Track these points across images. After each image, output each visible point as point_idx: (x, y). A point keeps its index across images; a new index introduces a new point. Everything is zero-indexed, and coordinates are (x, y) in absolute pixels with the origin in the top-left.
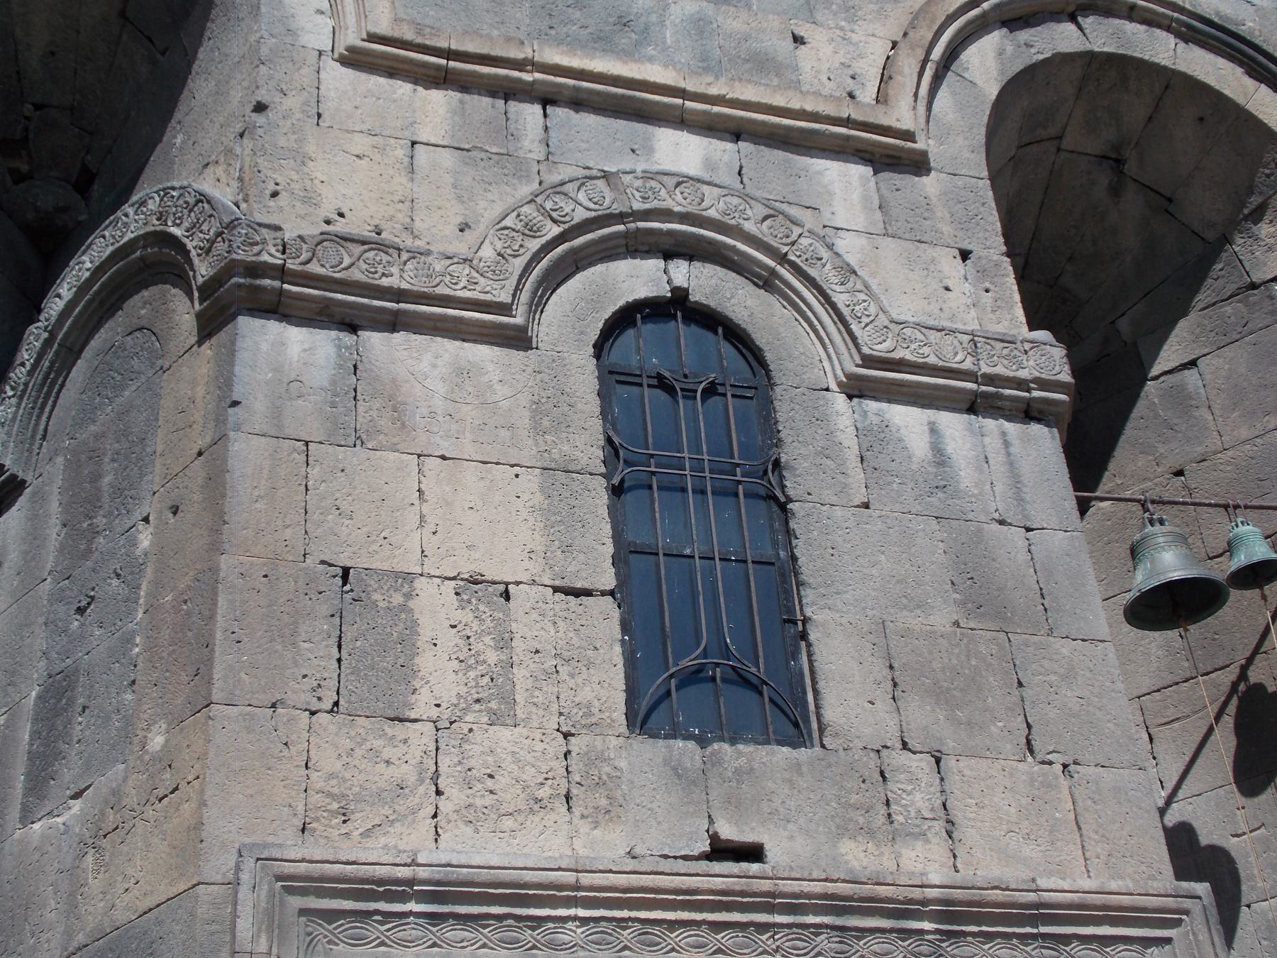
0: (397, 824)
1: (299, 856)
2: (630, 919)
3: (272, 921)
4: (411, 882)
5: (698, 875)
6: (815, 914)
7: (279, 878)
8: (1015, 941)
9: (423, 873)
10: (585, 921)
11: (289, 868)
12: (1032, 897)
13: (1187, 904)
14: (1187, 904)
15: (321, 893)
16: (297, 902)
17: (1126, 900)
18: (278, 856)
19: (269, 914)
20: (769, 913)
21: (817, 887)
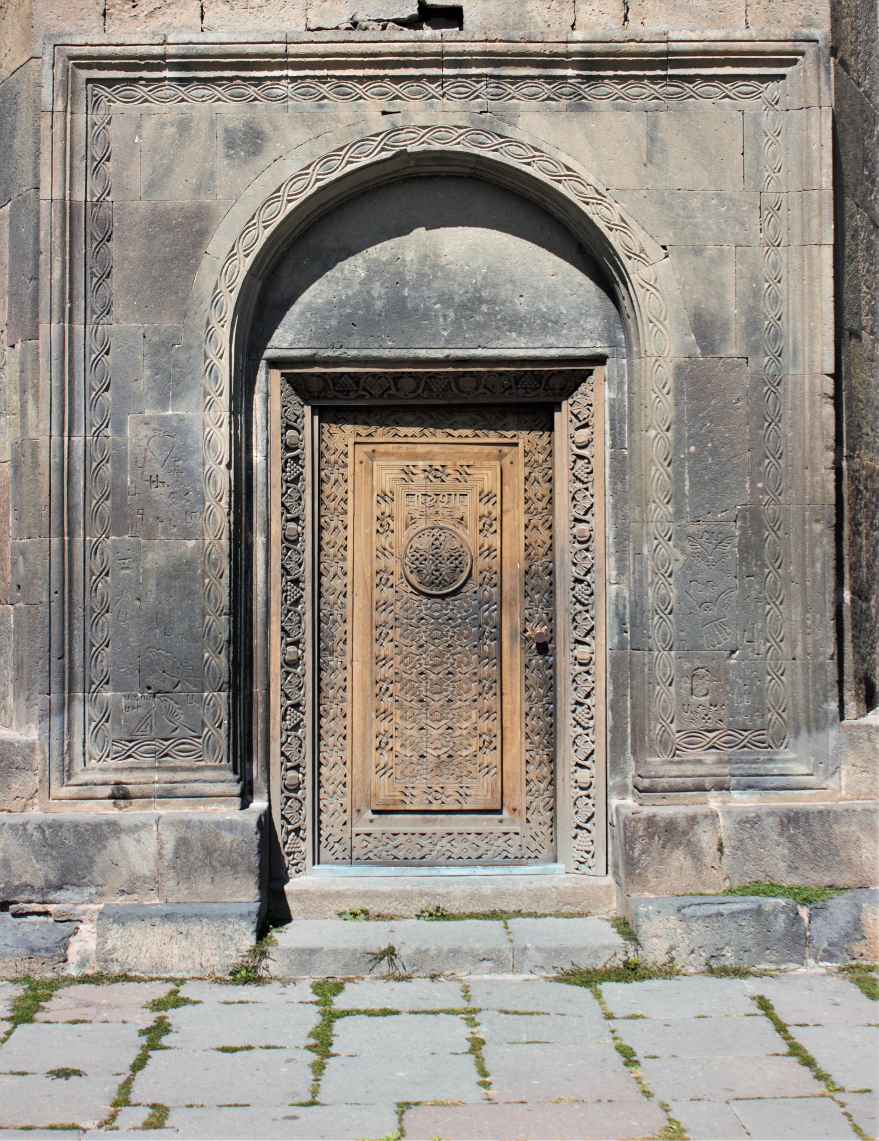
0: (173, 6)
1: (83, 42)
2: (328, 76)
3: (68, 91)
4: (164, 57)
5: (381, 41)
6: (477, 67)
7: (71, 58)
8: (646, 81)
9: (171, 50)
10: (294, 79)
11: (77, 51)
12: (662, 47)
13: (803, 46)
14: (803, 46)
15: (101, 67)
16: (84, 74)
17: (746, 46)
18: (69, 42)
19: (65, 84)
20: (439, 67)
21: (478, 47)
